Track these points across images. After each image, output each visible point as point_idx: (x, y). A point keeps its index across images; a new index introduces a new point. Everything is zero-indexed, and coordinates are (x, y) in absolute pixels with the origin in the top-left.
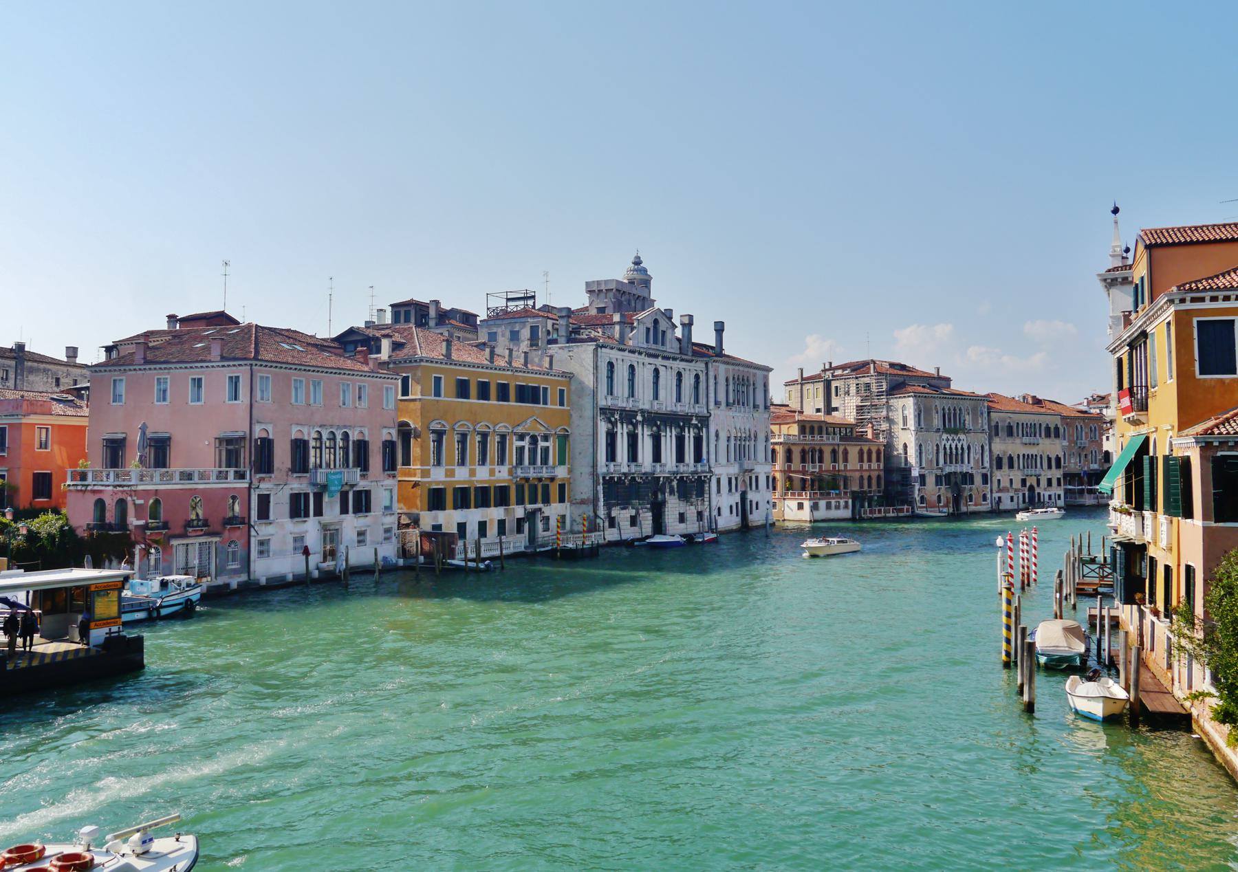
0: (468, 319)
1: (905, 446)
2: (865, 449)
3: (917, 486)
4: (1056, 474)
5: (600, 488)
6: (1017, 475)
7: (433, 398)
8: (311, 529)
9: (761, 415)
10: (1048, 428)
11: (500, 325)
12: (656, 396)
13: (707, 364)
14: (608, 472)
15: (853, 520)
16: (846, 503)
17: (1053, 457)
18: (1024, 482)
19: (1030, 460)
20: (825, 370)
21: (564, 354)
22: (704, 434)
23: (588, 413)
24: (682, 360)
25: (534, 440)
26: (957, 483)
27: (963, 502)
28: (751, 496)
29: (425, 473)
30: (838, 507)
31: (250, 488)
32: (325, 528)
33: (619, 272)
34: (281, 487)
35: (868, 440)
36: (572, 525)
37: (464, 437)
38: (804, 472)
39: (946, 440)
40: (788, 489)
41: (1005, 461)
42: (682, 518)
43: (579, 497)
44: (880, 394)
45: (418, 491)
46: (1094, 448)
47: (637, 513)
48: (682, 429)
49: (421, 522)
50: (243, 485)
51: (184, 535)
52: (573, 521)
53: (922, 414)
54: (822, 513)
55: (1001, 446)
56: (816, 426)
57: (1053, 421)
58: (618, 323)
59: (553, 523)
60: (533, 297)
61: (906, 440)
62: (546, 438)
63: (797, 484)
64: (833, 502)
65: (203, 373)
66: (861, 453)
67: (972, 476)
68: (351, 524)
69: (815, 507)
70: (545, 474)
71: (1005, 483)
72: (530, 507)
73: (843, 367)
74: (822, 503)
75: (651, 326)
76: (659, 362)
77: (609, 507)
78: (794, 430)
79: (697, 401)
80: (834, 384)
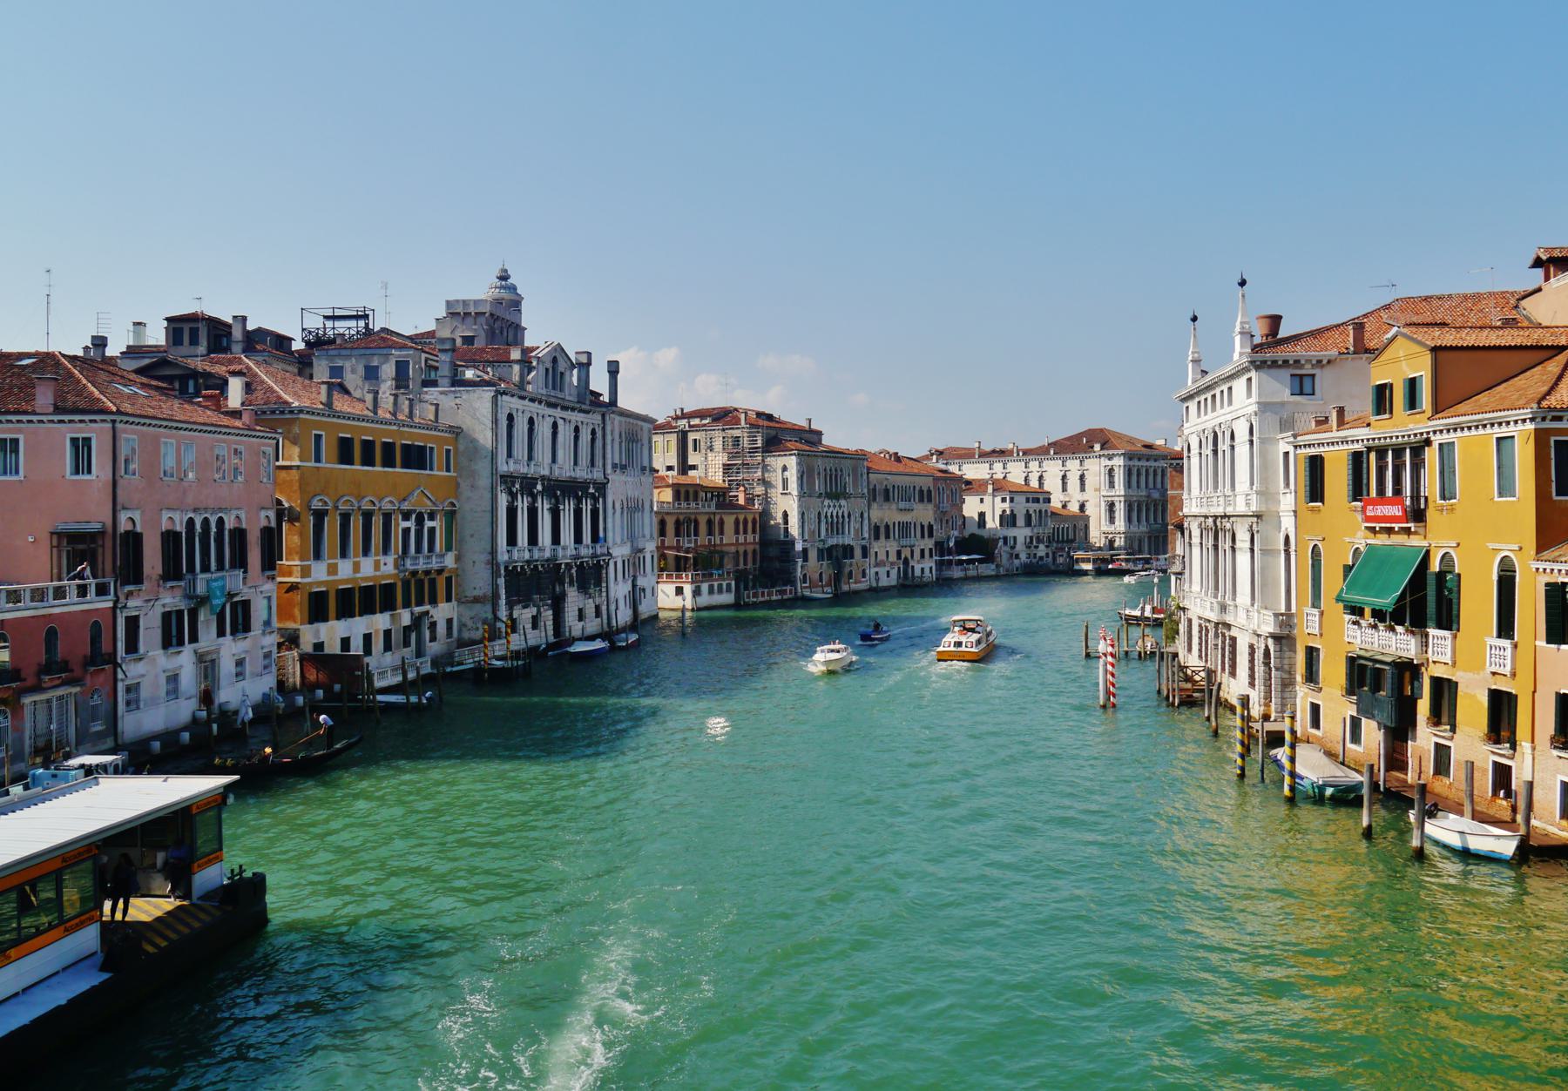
0: (282, 342)
1: (785, 515)
2: (741, 518)
3: (800, 562)
4: (928, 544)
5: (501, 581)
6: (892, 546)
7: (312, 464)
8: (185, 661)
9: (647, 479)
10: (921, 491)
11: (348, 357)
12: (554, 460)
13: (603, 416)
14: (511, 561)
15: (737, 606)
16: (729, 585)
17: (926, 524)
18: (899, 553)
19: (905, 529)
20: (677, 418)
21: (447, 402)
22: (601, 506)
23: (484, 481)
24: (581, 411)
25: (420, 521)
26: (837, 556)
27: (844, 579)
28: (641, 582)
29: (306, 572)
30: (720, 591)
31: (114, 608)
32: (200, 658)
34: (151, 604)
35: (742, 507)
36: (460, 631)
37: (345, 518)
38: (678, 548)
39: (829, 508)
40: (662, 570)
41: (882, 530)
42: (581, 616)
43: (471, 593)
44: (754, 450)
45: (297, 597)
46: (954, 512)
47: (539, 612)
48: (579, 501)
49: (302, 640)
50: (106, 603)
51: (37, 688)
52: (462, 625)
53: (805, 476)
54: (705, 599)
55: (883, 513)
56: (691, 491)
57: (926, 483)
58: (517, 362)
59: (441, 629)
60: (366, 317)
61: (787, 506)
62: (432, 518)
63: (671, 562)
65: (19, 431)
66: (737, 522)
67: (851, 548)
68: (229, 649)
69: (697, 592)
70: (434, 564)
71: (882, 556)
72: (418, 609)
73: (700, 414)
74: (705, 587)
75: (549, 365)
76: (558, 413)
77: (510, 605)
78: (667, 495)
79: (593, 465)
80: (691, 437)
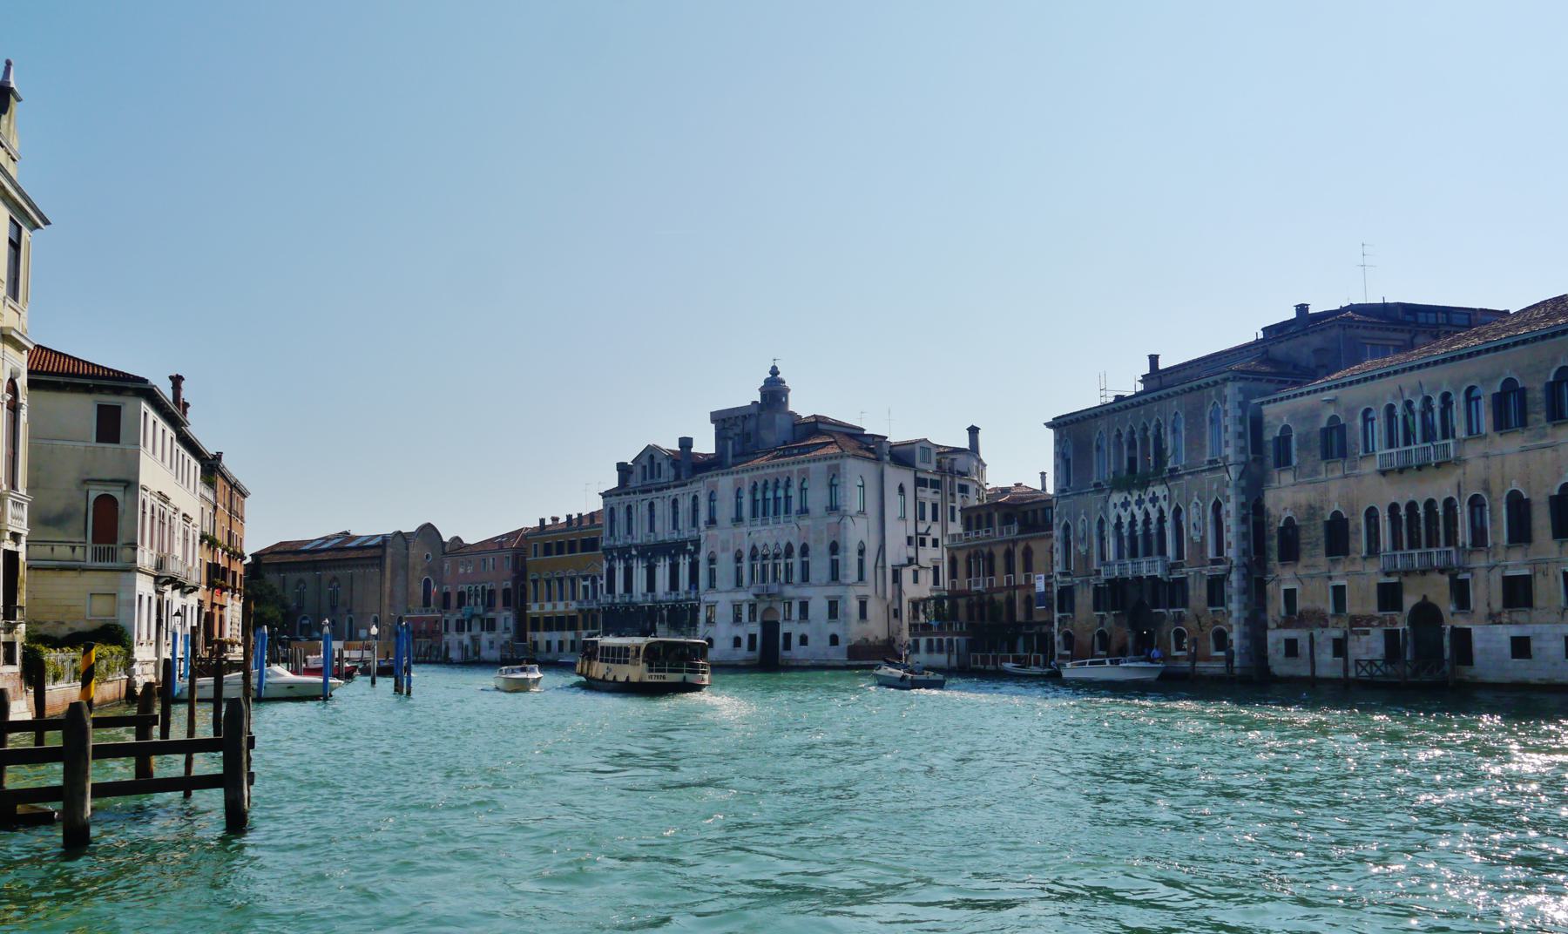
6: (1361, 578)
25: (594, 581)
30: (940, 650)
33: (746, 394)
64: (935, 638)
